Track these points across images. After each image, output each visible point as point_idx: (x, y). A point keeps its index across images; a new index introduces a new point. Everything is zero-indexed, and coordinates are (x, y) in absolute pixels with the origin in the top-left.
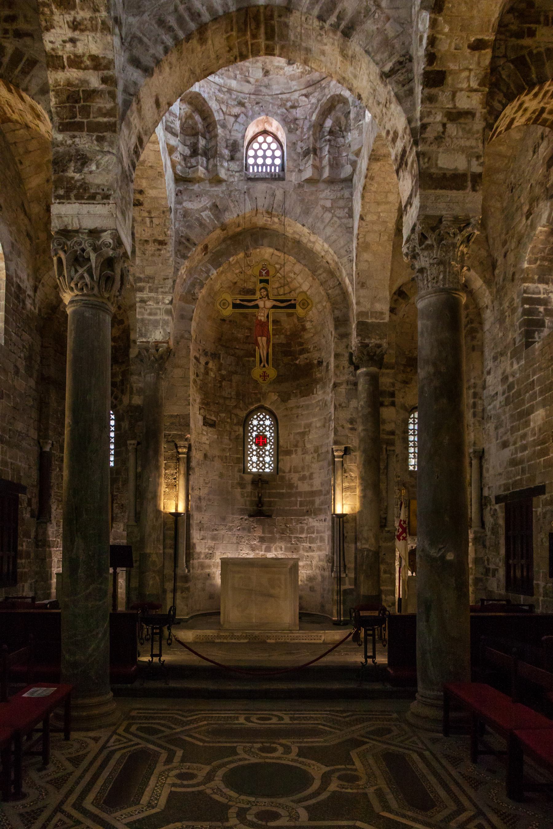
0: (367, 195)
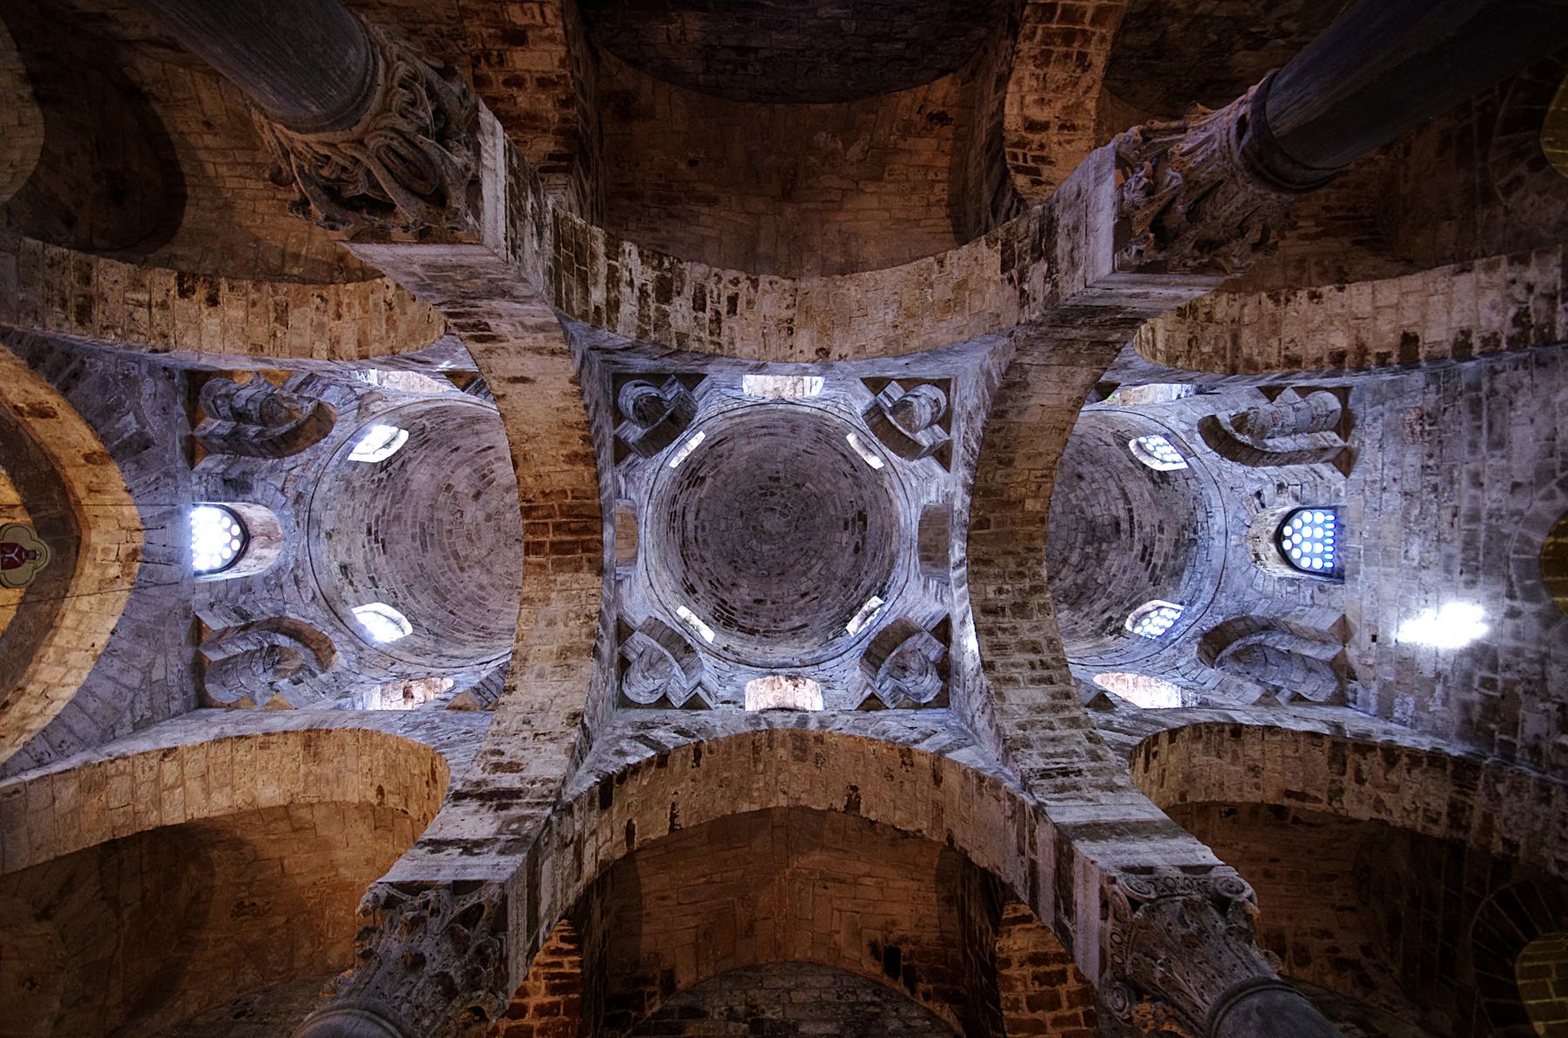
0: (227, 747)
